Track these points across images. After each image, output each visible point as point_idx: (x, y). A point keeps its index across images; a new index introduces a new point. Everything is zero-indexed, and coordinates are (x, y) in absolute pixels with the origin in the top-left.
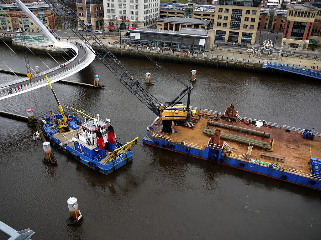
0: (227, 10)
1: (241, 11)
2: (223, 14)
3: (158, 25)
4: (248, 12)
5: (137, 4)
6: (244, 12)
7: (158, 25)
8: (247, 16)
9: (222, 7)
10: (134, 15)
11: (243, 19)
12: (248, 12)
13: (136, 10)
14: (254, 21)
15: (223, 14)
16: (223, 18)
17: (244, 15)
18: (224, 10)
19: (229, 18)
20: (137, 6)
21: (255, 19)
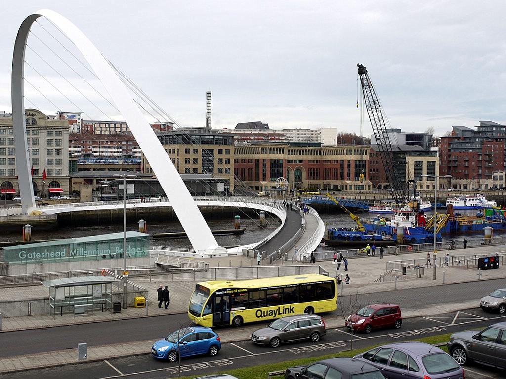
0: (196, 151)
1: (212, 151)
2: (191, 156)
3: (74, 183)
4: (220, 152)
5: (58, 148)
6: (216, 152)
7: (74, 183)
8: (220, 156)
9: (188, 147)
10: (54, 167)
11: (216, 162)
12: (220, 152)
13: (58, 157)
14: (229, 163)
15: (191, 156)
16: (191, 162)
17: (217, 156)
18: (191, 151)
19: (200, 161)
20: (58, 150)
21: (229, 159)
